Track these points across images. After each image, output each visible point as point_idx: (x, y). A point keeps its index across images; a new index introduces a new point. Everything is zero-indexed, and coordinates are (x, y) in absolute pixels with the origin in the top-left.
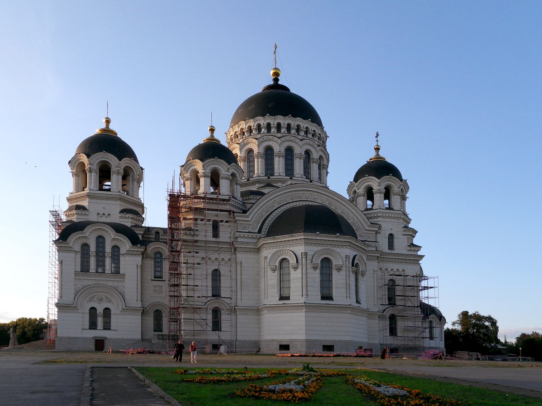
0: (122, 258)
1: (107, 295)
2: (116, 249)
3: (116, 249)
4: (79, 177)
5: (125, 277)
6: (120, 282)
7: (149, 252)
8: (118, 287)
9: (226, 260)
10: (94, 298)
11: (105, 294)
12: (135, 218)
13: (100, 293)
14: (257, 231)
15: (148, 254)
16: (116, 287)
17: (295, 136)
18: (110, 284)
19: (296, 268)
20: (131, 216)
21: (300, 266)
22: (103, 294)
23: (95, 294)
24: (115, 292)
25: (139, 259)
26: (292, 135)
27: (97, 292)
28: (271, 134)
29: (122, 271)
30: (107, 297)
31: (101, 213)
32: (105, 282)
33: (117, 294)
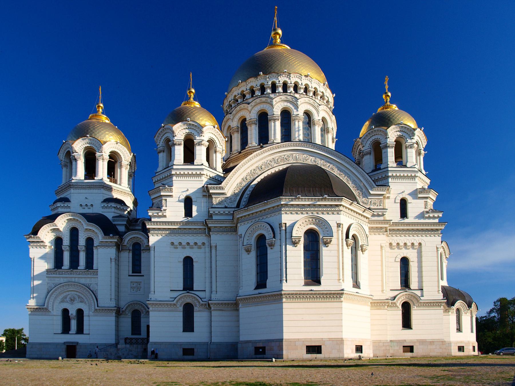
0: (95, 251)
1: (80, 295)
2: (90, 241)
3: (90, 241)
4: (67, 168)
5: (99, 273)
6: (93, 279)
7: (125, 244)
8: (91, 284)
9: (199, 244)
10: (66, 298)
11: (78, 294)
12: (118, 207)
13: (73, 292)
14: (235, 205)
15: (125, 245)
16: (88, 285)
17: (292, 95)
18: (83, 281)
19: (272, 245)
20: (113, 205)
21: (278, 242)
22: (75, 293)
23: (67, 293)
24: (87, 290)
25: (112, 252)
26: (288, 94)
27: (70, 291)
28: (264, 95)
29: (95, 267)
30: (79, 297)
31: (84, 204)
32: (76, 280)
33: (89, 292)
